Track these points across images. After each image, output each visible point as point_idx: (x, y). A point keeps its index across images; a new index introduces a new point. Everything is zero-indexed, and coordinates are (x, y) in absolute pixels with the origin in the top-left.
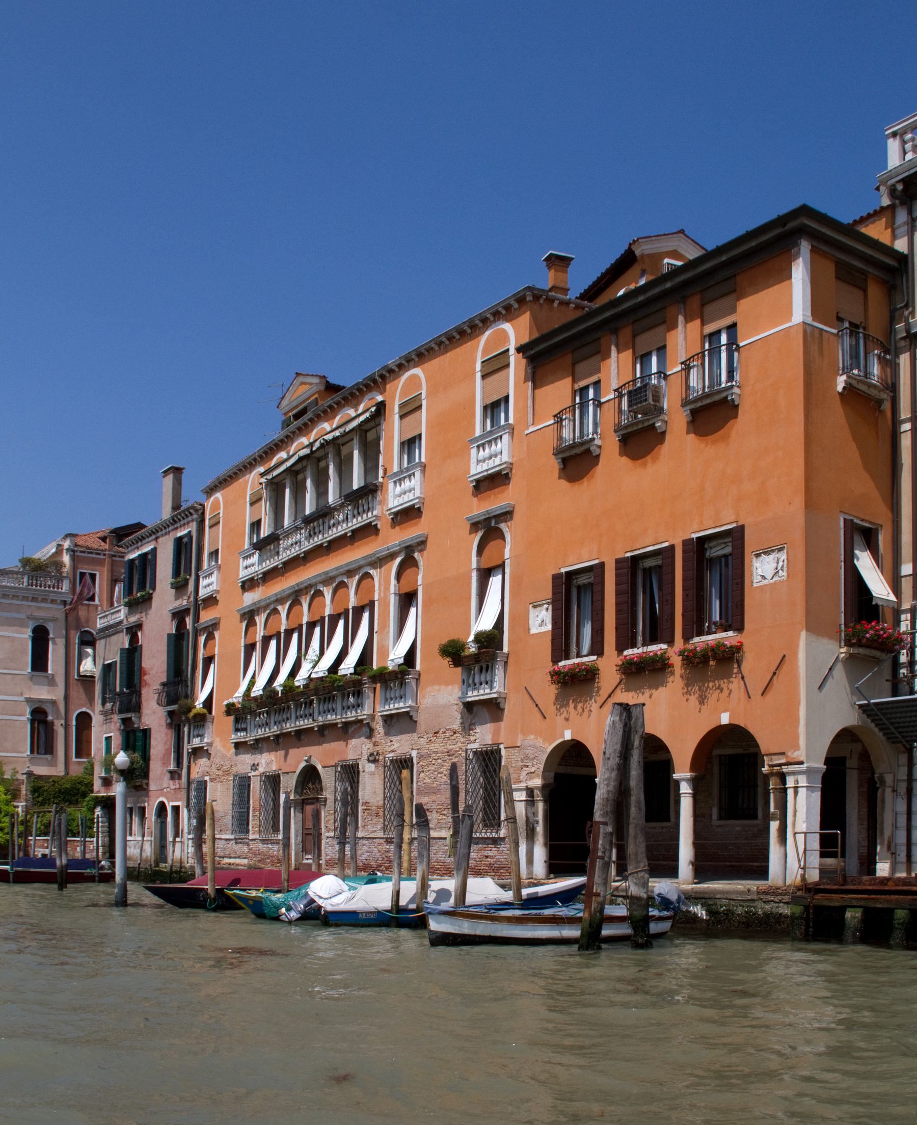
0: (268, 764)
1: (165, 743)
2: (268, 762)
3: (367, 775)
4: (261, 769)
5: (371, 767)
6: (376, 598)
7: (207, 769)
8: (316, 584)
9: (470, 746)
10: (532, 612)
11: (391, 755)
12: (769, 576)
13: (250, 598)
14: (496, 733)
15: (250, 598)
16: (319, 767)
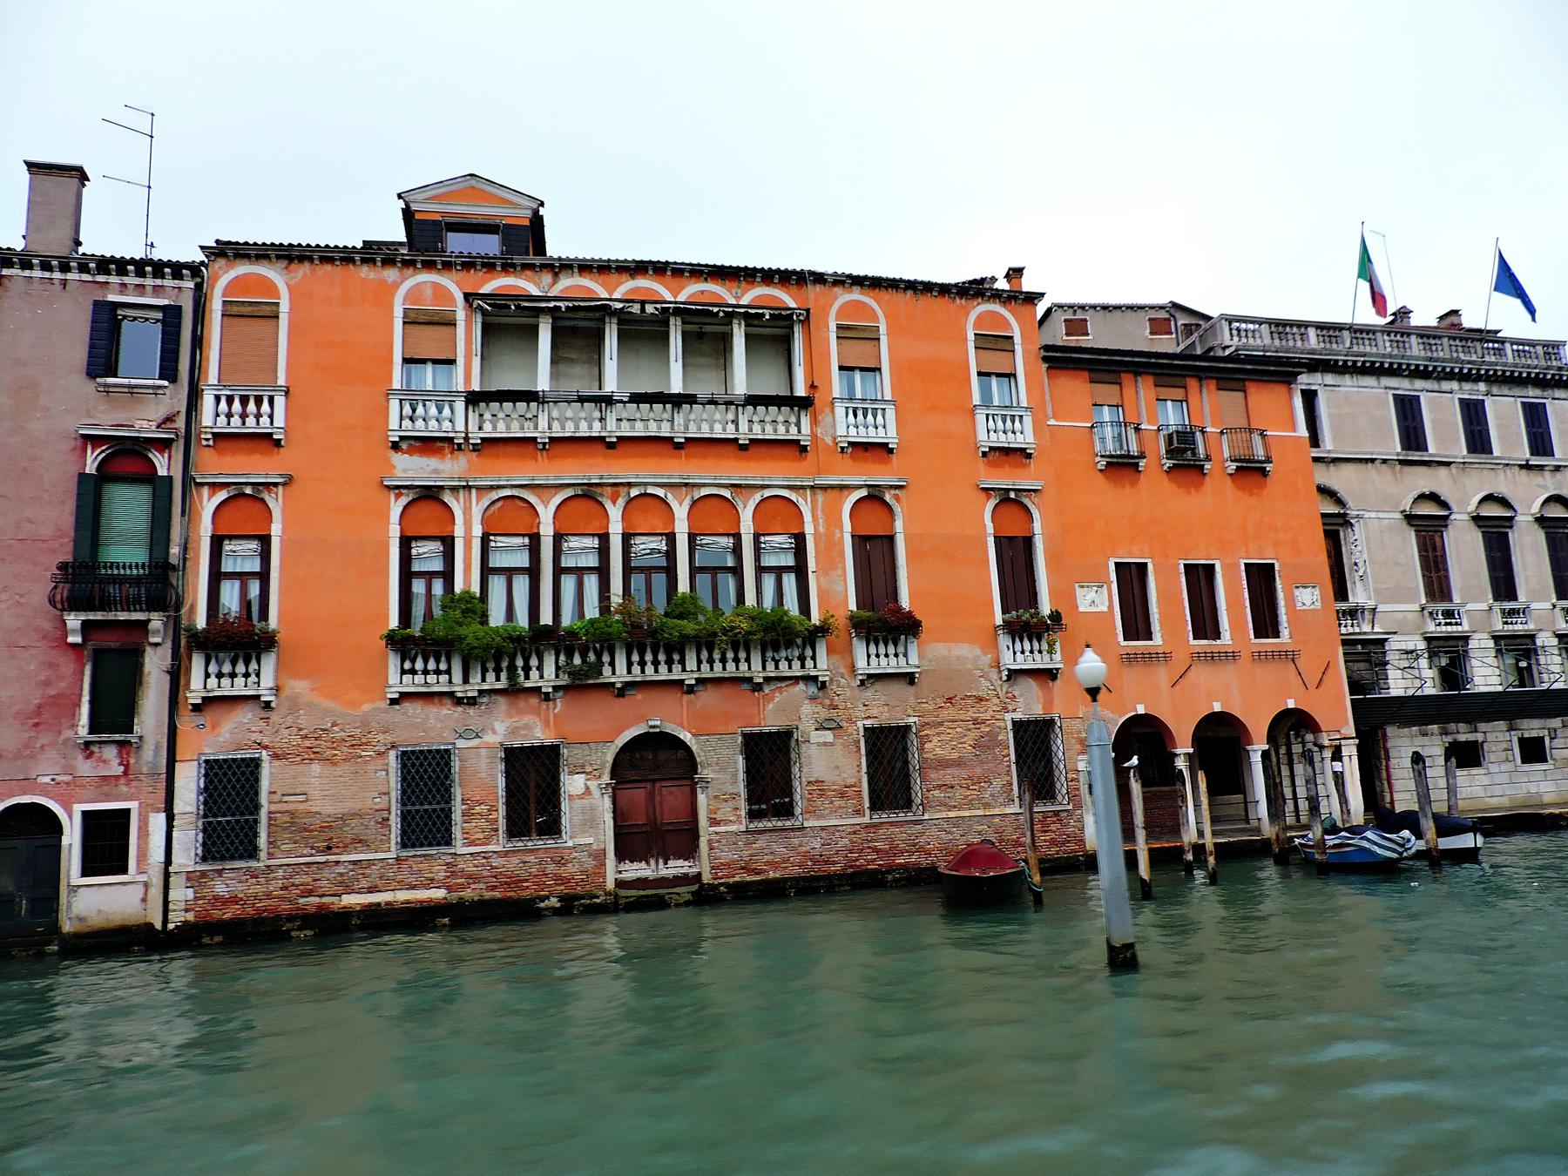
0: (514, 731)
1: (47, 683)
2: (505, 727)
3: (813, 747)
4: (491, 739)
5: (828, 736)
6: (809, 529)
7: (256, 737)
8: (646, 484)
9: (1008, 717)
10: (1079, 592)
11: (868, 723)
12: (1308, 603)
13: (413, 469)
14: (1048, 703)
15: (413, 469)
16: (686, 736)
